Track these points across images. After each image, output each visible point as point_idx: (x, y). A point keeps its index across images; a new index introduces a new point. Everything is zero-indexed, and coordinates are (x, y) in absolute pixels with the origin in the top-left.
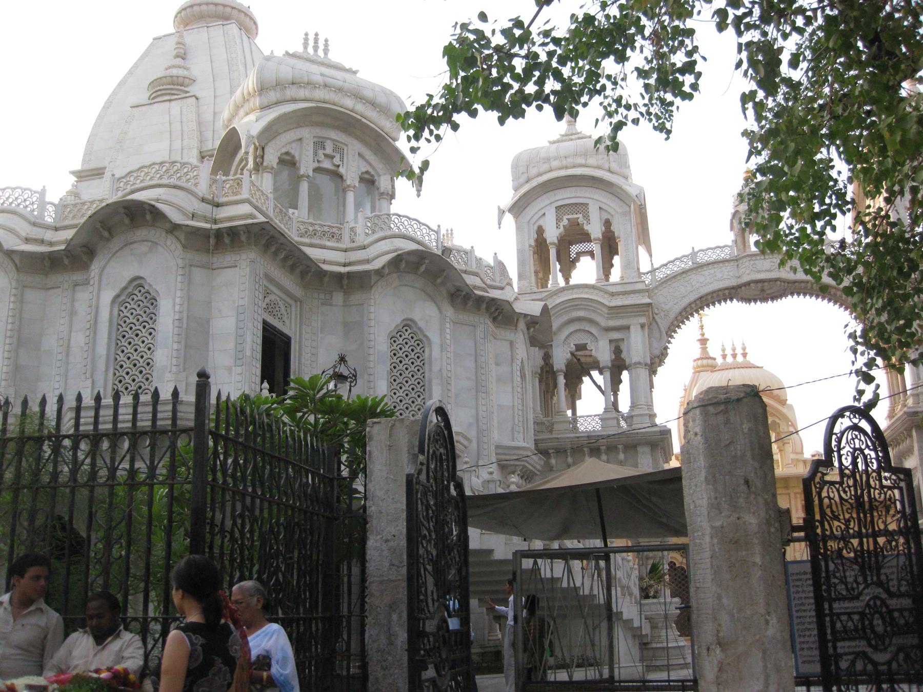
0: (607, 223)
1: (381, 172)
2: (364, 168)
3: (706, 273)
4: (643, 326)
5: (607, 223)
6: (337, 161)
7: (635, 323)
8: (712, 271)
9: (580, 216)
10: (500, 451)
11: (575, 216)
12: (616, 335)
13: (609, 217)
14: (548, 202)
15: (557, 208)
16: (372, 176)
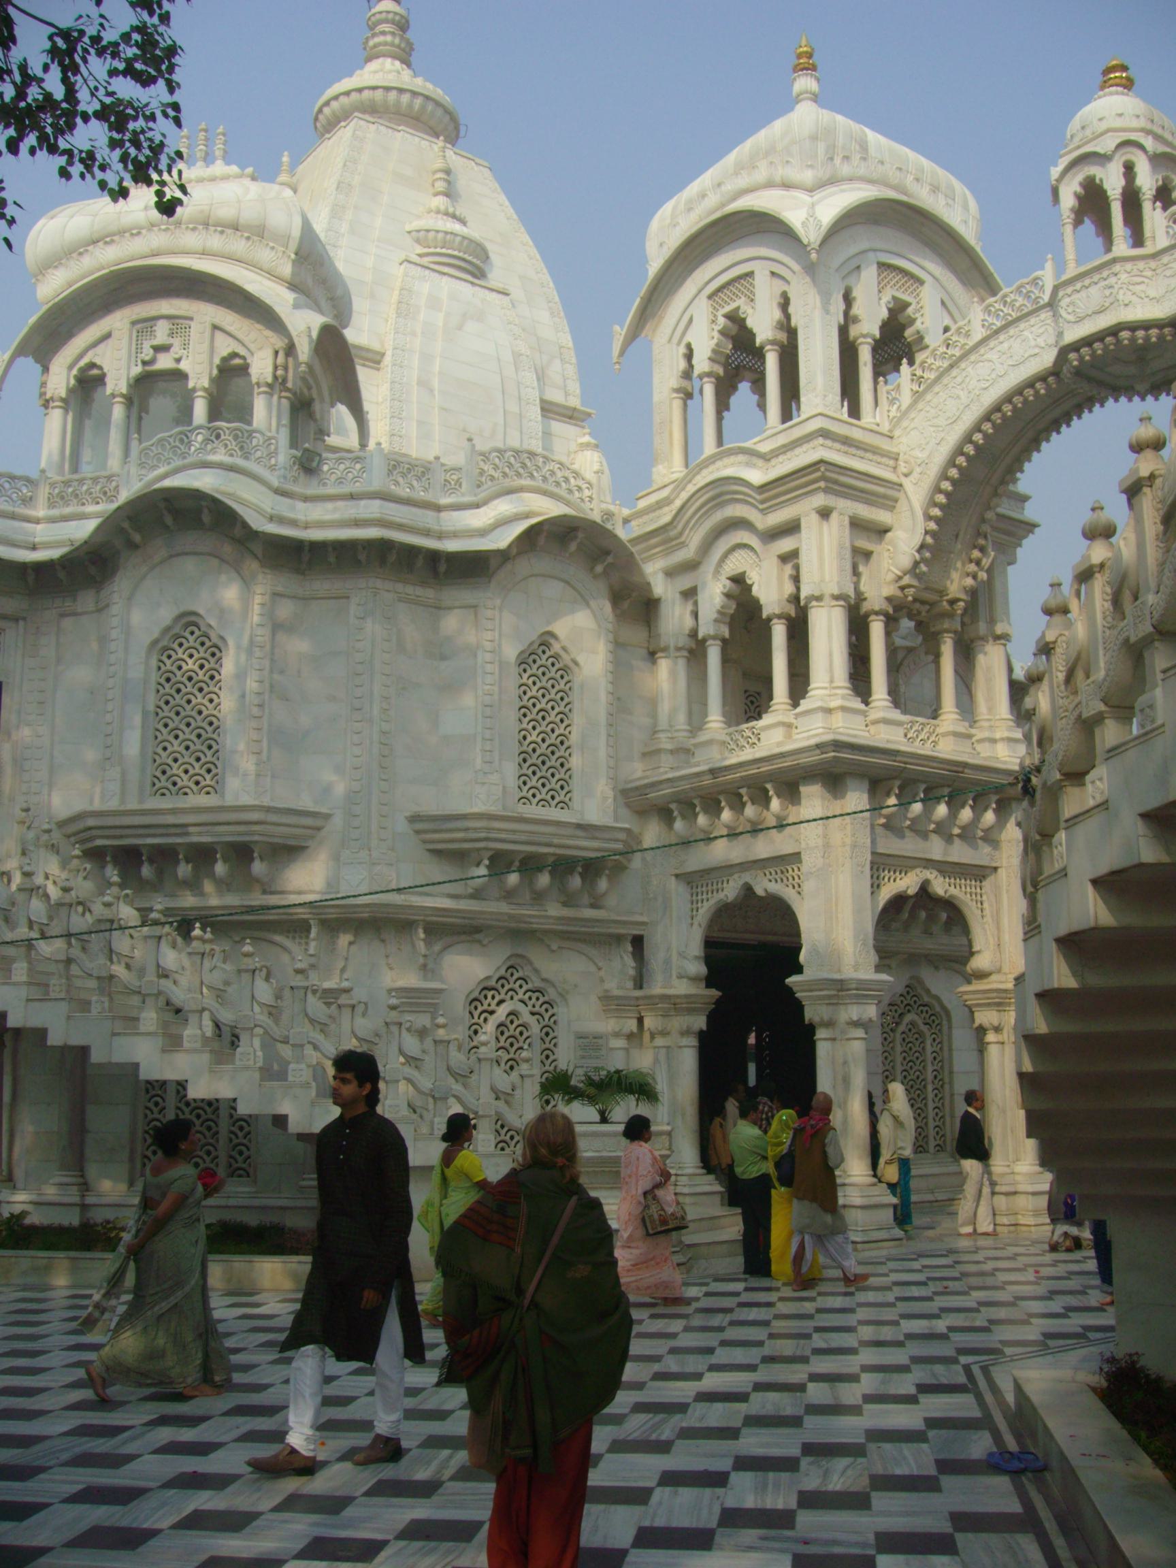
0: (785, 303)
1: (252, 347)
2: (225, 347)
3: (992, 355)
4: (825, 513)
5: (785, 303)
6: (177, 351)
7: (805, 509)
8: (1006, 345)
9: (741, 302)
10: (420, 826)
11: (733, 306)
12: (786, 545)
13: (786, 288)
14: (694, 291)
15: (710, 297)
16: (244, 358)
